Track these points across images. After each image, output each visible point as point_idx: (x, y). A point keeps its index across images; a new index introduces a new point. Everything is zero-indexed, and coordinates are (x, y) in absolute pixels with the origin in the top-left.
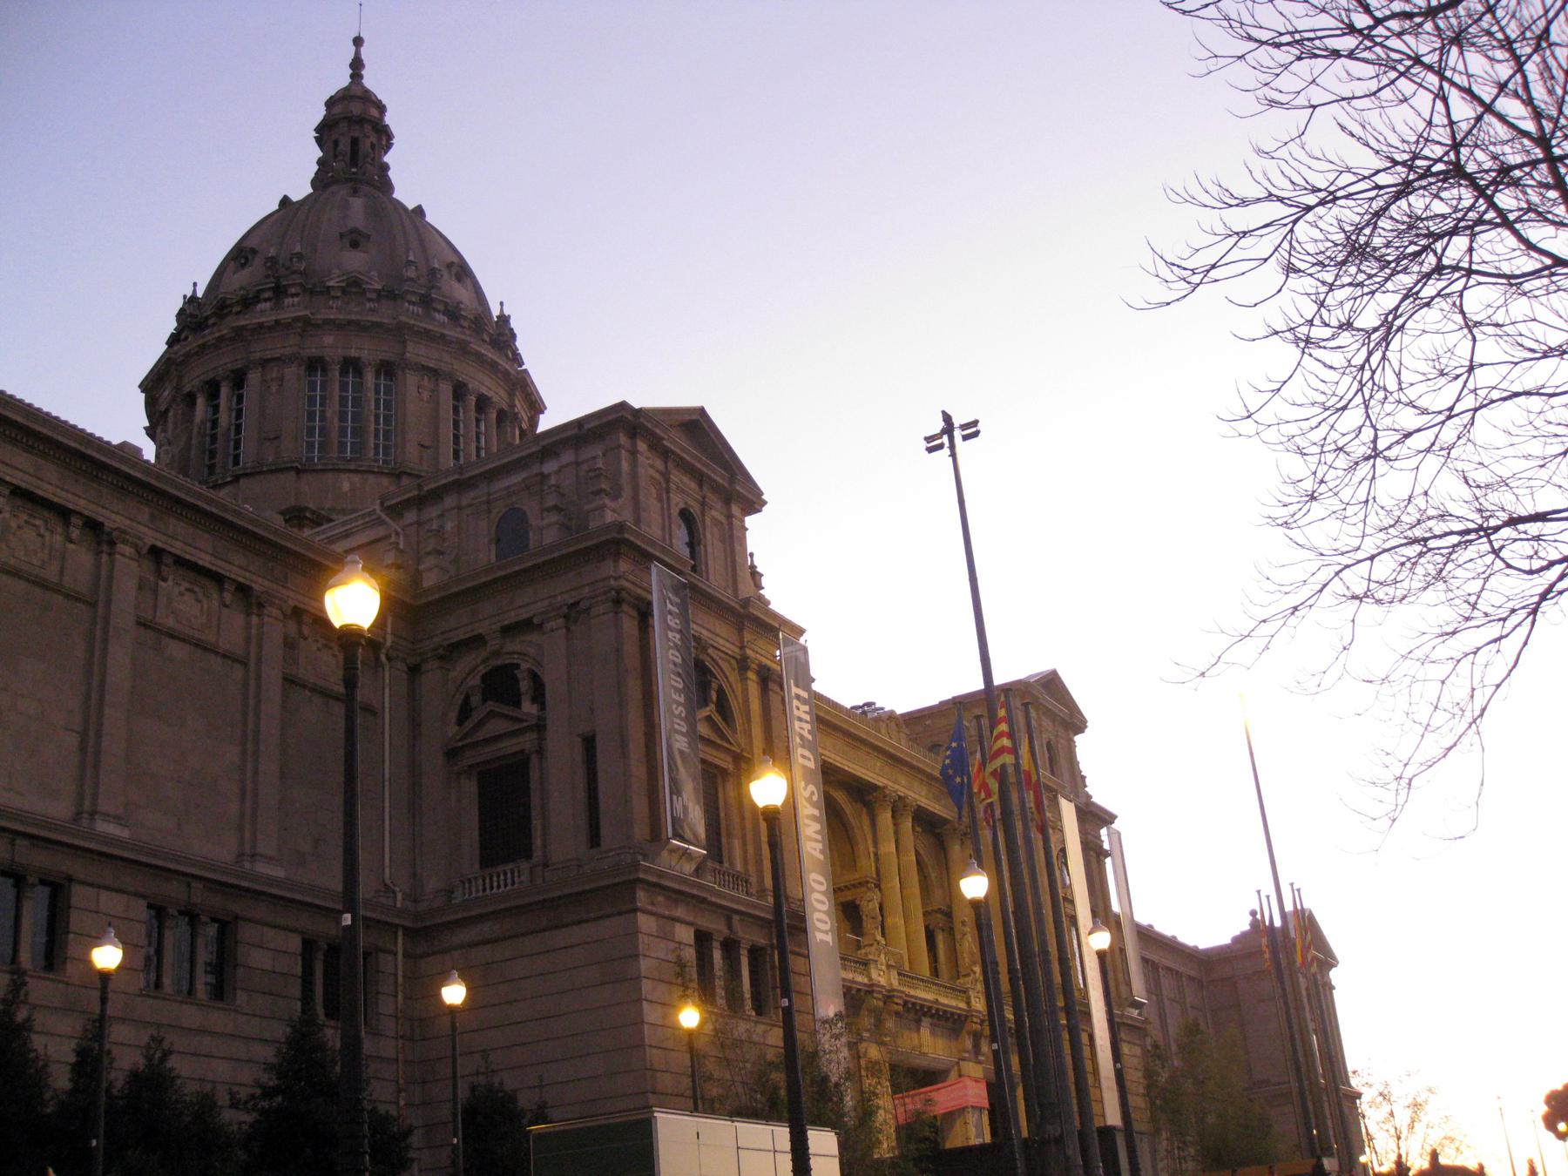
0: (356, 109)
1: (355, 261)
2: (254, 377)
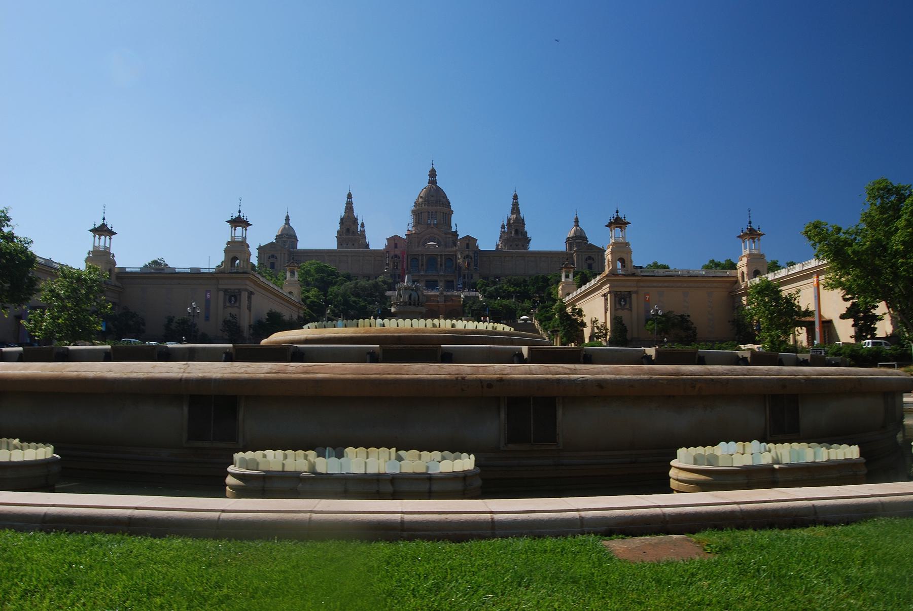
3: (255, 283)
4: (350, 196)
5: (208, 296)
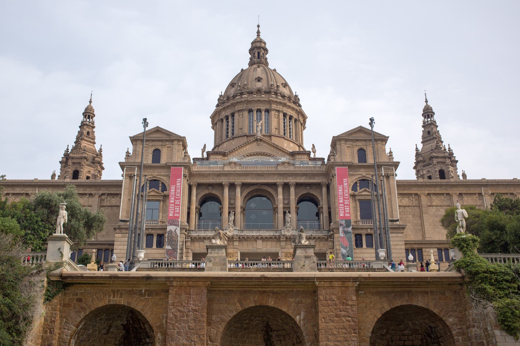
0: (258, 45)
2: (236, 115)
4: (89, 114)
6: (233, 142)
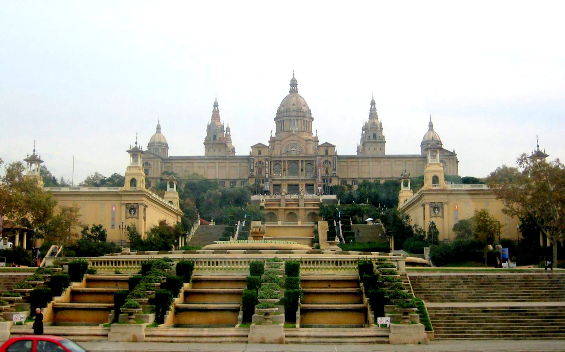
1: (294, 107)
3: (148, 198)
4: (216, 105)
5: (114, 209)
6: (284, 133)
